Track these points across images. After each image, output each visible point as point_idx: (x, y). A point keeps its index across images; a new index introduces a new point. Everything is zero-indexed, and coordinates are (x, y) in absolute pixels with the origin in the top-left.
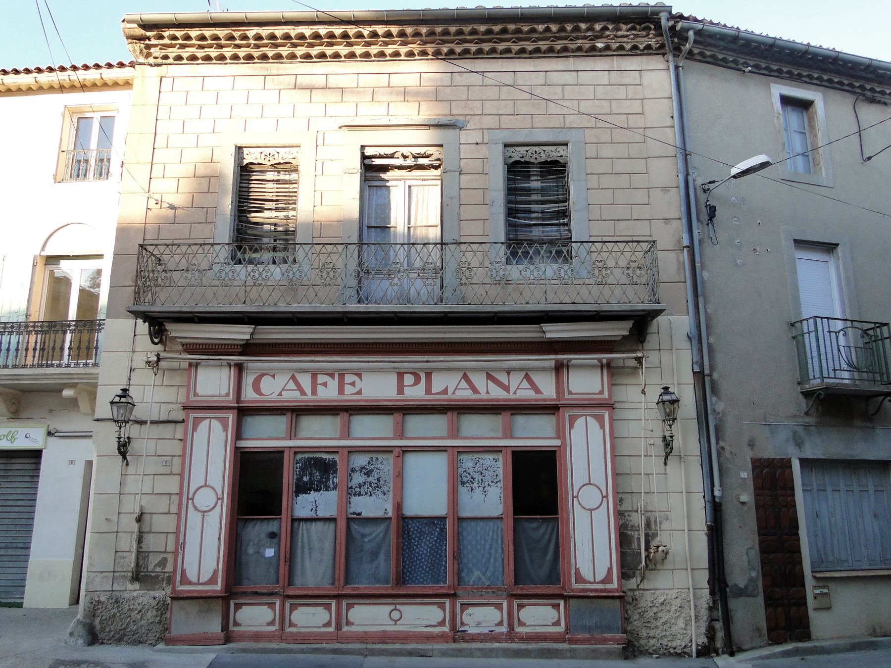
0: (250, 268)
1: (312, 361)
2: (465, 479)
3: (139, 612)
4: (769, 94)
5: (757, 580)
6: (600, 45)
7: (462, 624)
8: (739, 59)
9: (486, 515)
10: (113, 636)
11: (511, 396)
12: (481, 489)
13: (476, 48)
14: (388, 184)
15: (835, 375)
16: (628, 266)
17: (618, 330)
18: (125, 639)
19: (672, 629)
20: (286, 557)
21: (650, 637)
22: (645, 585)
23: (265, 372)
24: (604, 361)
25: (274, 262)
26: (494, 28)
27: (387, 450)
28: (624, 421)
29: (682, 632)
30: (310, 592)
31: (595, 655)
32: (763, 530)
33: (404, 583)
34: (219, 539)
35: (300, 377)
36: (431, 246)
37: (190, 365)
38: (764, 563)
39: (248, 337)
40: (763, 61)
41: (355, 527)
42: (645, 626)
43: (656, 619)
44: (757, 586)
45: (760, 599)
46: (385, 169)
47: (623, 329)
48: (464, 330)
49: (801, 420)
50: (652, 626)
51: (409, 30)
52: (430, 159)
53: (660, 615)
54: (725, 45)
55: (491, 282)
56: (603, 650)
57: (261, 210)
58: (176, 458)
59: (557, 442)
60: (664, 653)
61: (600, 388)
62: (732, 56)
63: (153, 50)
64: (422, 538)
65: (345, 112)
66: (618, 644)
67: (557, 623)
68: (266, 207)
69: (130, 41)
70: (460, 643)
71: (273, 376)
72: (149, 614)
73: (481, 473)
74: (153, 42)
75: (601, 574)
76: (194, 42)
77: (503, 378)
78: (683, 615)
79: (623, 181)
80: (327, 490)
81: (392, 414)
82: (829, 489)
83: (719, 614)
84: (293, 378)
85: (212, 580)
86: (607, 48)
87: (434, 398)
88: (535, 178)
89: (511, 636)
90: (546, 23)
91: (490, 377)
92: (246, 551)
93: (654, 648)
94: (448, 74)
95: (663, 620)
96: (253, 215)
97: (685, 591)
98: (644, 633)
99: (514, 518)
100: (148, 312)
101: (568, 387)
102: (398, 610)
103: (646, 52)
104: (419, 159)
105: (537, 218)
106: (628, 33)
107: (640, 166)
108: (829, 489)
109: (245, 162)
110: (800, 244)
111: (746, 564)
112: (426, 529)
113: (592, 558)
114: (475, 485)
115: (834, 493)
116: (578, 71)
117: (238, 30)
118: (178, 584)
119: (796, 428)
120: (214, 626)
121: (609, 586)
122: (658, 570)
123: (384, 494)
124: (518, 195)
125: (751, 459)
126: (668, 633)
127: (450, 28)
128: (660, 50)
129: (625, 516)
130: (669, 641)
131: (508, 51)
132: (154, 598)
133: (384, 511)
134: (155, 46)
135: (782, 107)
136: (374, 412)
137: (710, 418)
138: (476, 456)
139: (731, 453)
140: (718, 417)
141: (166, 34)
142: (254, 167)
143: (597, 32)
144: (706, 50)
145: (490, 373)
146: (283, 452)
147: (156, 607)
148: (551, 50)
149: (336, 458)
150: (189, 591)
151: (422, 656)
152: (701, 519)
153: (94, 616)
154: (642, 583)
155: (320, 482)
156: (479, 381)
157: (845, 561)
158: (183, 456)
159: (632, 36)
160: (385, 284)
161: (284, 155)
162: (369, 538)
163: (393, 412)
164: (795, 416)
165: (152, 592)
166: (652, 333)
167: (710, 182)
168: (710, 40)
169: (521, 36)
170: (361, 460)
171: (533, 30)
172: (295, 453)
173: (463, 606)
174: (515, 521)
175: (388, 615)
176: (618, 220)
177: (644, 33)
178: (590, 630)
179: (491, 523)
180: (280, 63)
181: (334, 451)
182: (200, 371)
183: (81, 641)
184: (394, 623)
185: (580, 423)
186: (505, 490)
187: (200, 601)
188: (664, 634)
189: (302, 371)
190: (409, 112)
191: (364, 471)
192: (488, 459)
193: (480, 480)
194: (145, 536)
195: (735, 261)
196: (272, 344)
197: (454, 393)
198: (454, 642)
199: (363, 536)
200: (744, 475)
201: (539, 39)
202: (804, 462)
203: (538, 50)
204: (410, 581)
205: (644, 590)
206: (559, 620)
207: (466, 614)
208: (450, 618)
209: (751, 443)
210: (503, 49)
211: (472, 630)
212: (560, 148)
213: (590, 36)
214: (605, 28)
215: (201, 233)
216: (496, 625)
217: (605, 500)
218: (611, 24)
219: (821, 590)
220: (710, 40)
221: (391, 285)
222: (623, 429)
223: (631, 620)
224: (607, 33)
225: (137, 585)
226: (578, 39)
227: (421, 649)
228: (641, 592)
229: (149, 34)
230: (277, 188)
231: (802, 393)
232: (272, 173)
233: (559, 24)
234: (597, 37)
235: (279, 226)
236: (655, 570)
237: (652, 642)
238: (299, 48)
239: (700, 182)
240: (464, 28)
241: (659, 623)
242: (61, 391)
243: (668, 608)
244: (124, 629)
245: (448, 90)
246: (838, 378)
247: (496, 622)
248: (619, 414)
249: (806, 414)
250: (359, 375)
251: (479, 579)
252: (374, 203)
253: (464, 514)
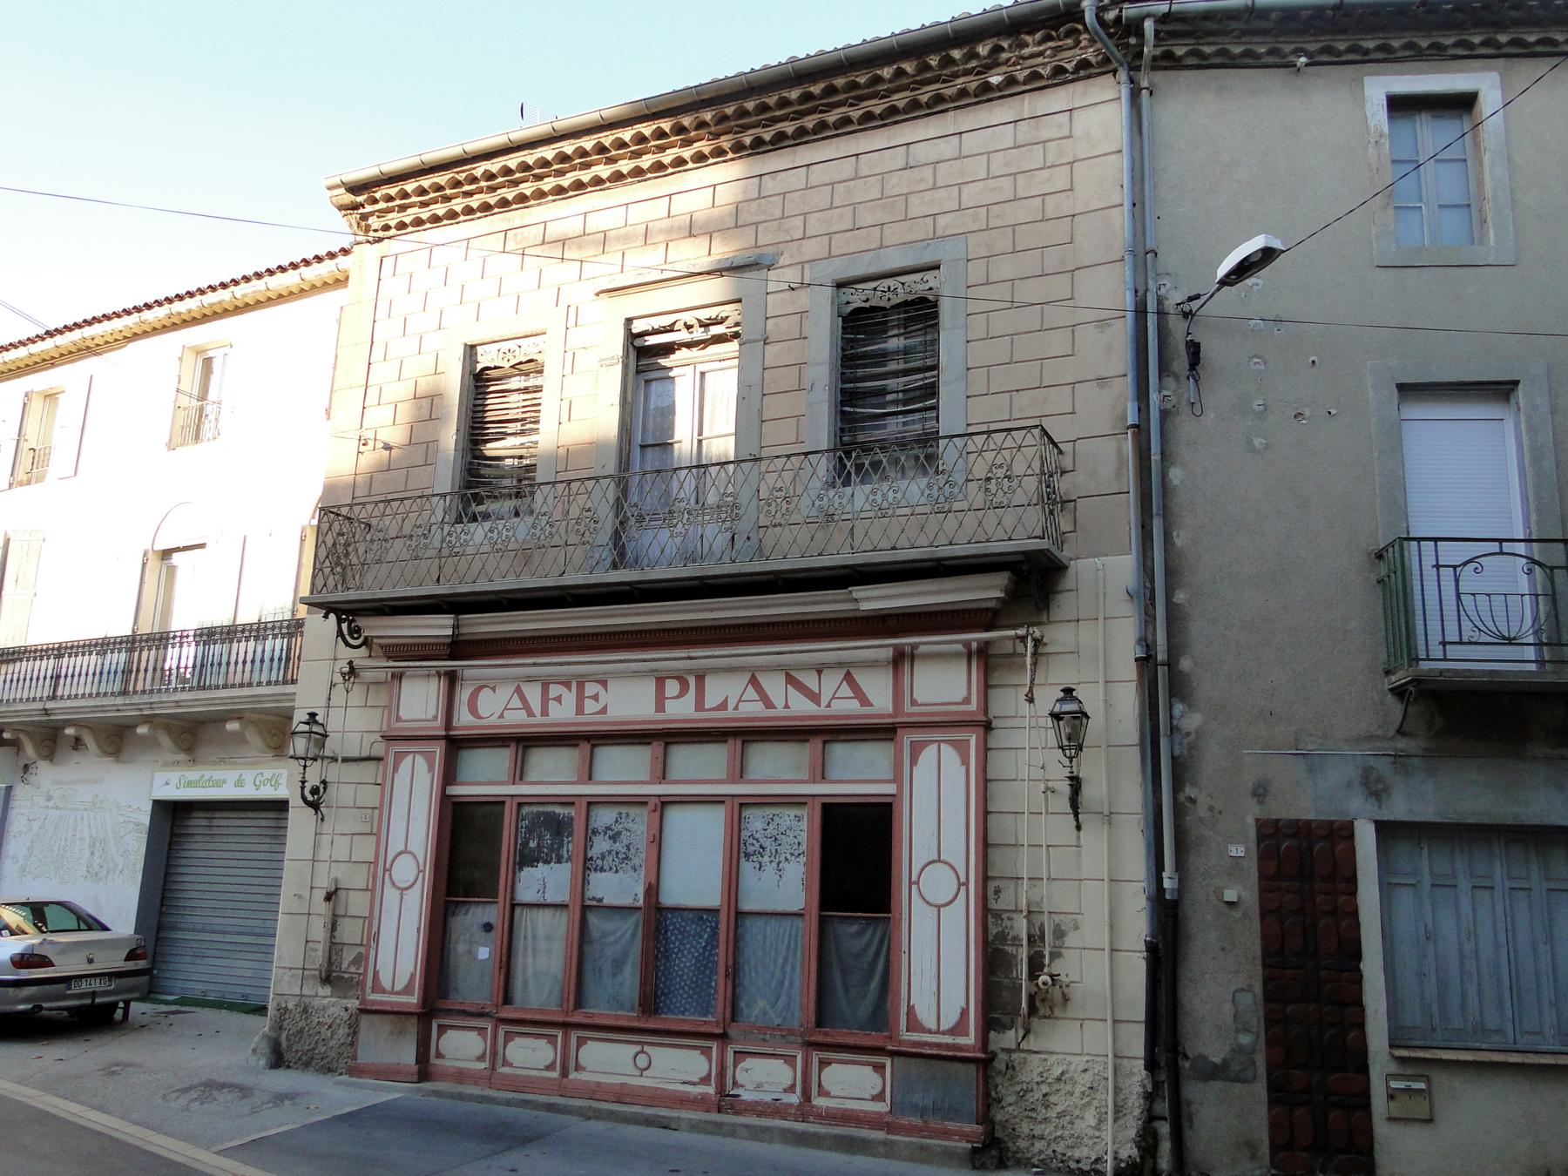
0: (487, 525)
1: (535, 664)
2: (751, 849)
3: (330, 1027)
4: (1360, 101)
5: (1253, 1051)
6: (995, 80)
7: (735, 1083)
8: (1281, 46)
9: (780, 908)
10: (300, 1059)
11: (822, 710)
12: (774, 865)
13: (793, 128)
14: (671, 374)
15: (1445, 654)
16: (989, 475)
17: (987, 590)
18: (314, 1064)
19: (1075, 1126)
20: (501, 960)
21: (1034, 1136)
22: (1032, 1043)
23: (483, 683)
24: (974, 645)
25: (517, 514)
26: (812, 89)
27: (638, 802)
28: (1008, 752)
29: (1091, 1132)
30: (529, 1017)
31: (924, 1156)
32: (1275, 956)
33: (656, 1011)
34: (419, 929)
35: (526, 688)
36: (731, 467)
37: (393, 676)
38: (1270, 1021)
39: (449, 632)
40: (1339, 37)
41: (594, 920)
42: (1027, 1117)
43: (1047, 1107)
44: (1253, 1063)
45: (1260, 1089)
46: (668, 349)
47: (993, 587)
48: (740, 604)
49: (1390, 744)
50: (1039, 1118)
51: (687, 121)
52: (727, 323)
53: (1053, 1099)
54: (1245, 27)
55: (768, 524)
56: (938, 1149)
57: (503, 436)
59: (890, 789)
60: (1059, 1169)
61: (964, 693)
62: (1263, 43)
63: (371, 220)
64: (685, 942)
65: (606, 270)
66: (968, 1141)
67: (879, 1097)
68: (509, 431)
69: (343, 212)
70: (727, 1113)
71: (494, 689)
72: (341, 1031)
73: (776, 839)
74: (369, 208)
75: (950, 1019)
76: (414, 199)
77: (810, 680)
78: (1095, 1103)
79: (1030, 318)
80: (559, 862)
81: (650, 743)
82: (1464, 885)
83: (1162, 1107)
84: (518, 691)
85: (407, 990)
86: (1011, 81)
87: (709, 717)
88: (896, 332)
89: (804, 1111)
90: (894, 62)
91: (790, 680)
92: (455, 949)
93: (1043, 1156)
94: (755, 179)
95: (1059, 1109)
96: (489, 445)
97: (1100, 1059)
98: (1025, 1128)
99: (820, 916)
100: (332, 603)
101: (912, 695)
102: (645, 1053)
103: (1082, 73)
104: (711, 328)
105: (895, 402)
106: (1041, 48)
107: (1060, 286)
108: (1464, 885)
109: (479, 367)
110: (1409, 391)
111: (1230, 1020)
112: (692, 928)
113: (935, 990)
114: (766, 859)
115: (1480, 893)
116: (961, 133)
117: (463, 172)
118: (368, 990)
119: (1372, 762)
120: (407, 1055)
121: (961, 1040)
122: (1056, 1018)
123: (635, 870)
124: (858, 367)
125: (1257, 820)
126: (1067, 1133)
127: (745, 104)
128: (1105, 66)
129: (1002, 920)
130: (1068, 1147)
131: (846, 121)
132: (347, 1009)
133: (633, 896)
134: (372, 214)
135: (1390, 118)
136: (701, 739)
137: (1164, 743)
138: (769, 811)
139: (1211, 808)
140: (1186, 741)
141: (378, 195)
142: (493, 373)
143: (985, 58)
144: (1202, 44)
145: (792, 673)
146: (503, 803)
148: (915, 105)
149: (571, 811)
150: (380, 1003)
151: (665, 1128)
152: (1137, 926)
153: (281, 1028)
154: (1026, 1040)
155: (551, 849)
156: (775, 686)
157: (1496, 1032)
158: (380, 808)
159: (1048, 52)
160: (665, 534)
161: (527, 350)
162: (612, 938)
163: (576, 742)
164: (1371, 736)
165: (344, 1001)
166: (1068, 591)
167: (1191, 299)
168: (1209, 25)
169: (860, 92)
170: (604, 817)
171: (878, 80)
172: (520, 805)
173: (738, 1055)
174: (823, 922)
175: (631, 1061)
176: (1017, 391)
177: (1069, 41)
178: (923, 1112)
179: (788, 922)
180: (525, 207)
181: (568, 801)
182: (406, 685)
183: (263, 1062)
184: (638, 1073)
185: (928, 755)
186: (808, 873)
187: (393, 1017)
188: (1059, 1133)
189: (530, 680)
190: (695, 254)
191: (610, 833)
192: (788, 816)
193: (773, 851)
194: (340, 921)
195: (1250, 442)
196: (485, 641)
197: (736, 708)
198: (719, 1112)
199: (604, 935)
200: (1237, 850)
201: (890, 92)
202: (1386, 830)
203: (893, 110)
204: (666, 1010)
205: (1029, 1052)
206: (883, 1091)
207: (742, 1069)
208: (717, 1075)
209: (1261, 791)
210: (795, 131)
211: (746, 1096)
212: (929, 275)
213: (974, 68)
214: (997, 49)
215: (420, 479)
216: (785, 1091)
217: (963, 888)
218: (1004, 39)
219: (1408, 1083)
220: (1209, 25)
221: (672, 536)
222: (1001, 765)
223: (1003, 1103)
224: (1004, 56)
225: (328, 990)
226: (958, 77)
227: (664, 1117)
228: (1023, 1055)
229: (360, 199)
230: (524, 400)
231: (1391, 690)
232: (518, 378)
233: (916, 59)
234: (987, 68)
235: (526, 458)
236: (1049, 1017)
237: (1039, 1145)
238: (546, 180)
239: (1175, 298)
240: (766, 100)
241: (1052, 1114)
242: (64, 728)
243: (1068, 1088)
244: (314, 1049)
245: (754, 205)
246: (1432, 660)
247: (785, 1086)
248: (996, 740)
249: (1400, 732)
250: (604, 683)
251: (765, 1013)
252: (652, 407)
253: (746, 906)
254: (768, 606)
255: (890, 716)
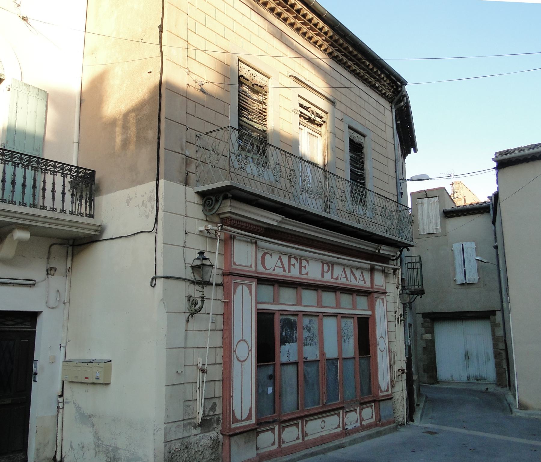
58: (219, 316)
59: (370, 313)
71: (271, 255)
80: (293, 342)
84: (280, 258)
85: (249, 417)
132: (211, 438)
146: (274, 314)
147: (212, 446)
182: (236, 243)
250: (307, 261)
254: (351, 241)
255: (369, 288)
